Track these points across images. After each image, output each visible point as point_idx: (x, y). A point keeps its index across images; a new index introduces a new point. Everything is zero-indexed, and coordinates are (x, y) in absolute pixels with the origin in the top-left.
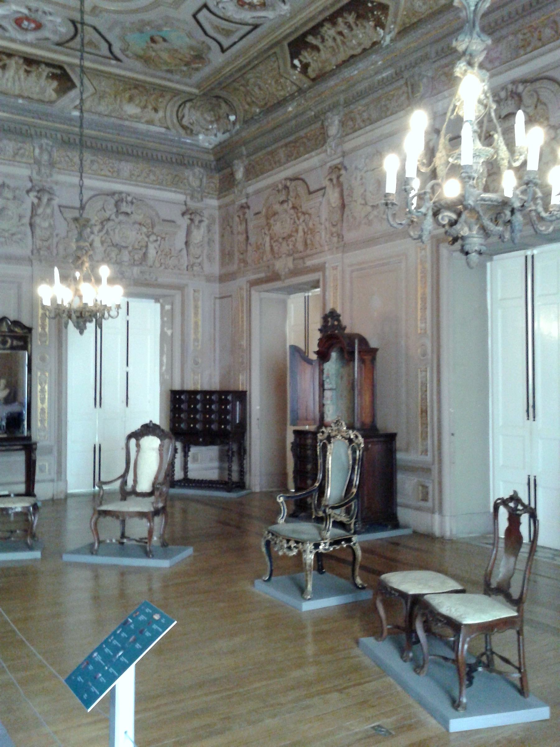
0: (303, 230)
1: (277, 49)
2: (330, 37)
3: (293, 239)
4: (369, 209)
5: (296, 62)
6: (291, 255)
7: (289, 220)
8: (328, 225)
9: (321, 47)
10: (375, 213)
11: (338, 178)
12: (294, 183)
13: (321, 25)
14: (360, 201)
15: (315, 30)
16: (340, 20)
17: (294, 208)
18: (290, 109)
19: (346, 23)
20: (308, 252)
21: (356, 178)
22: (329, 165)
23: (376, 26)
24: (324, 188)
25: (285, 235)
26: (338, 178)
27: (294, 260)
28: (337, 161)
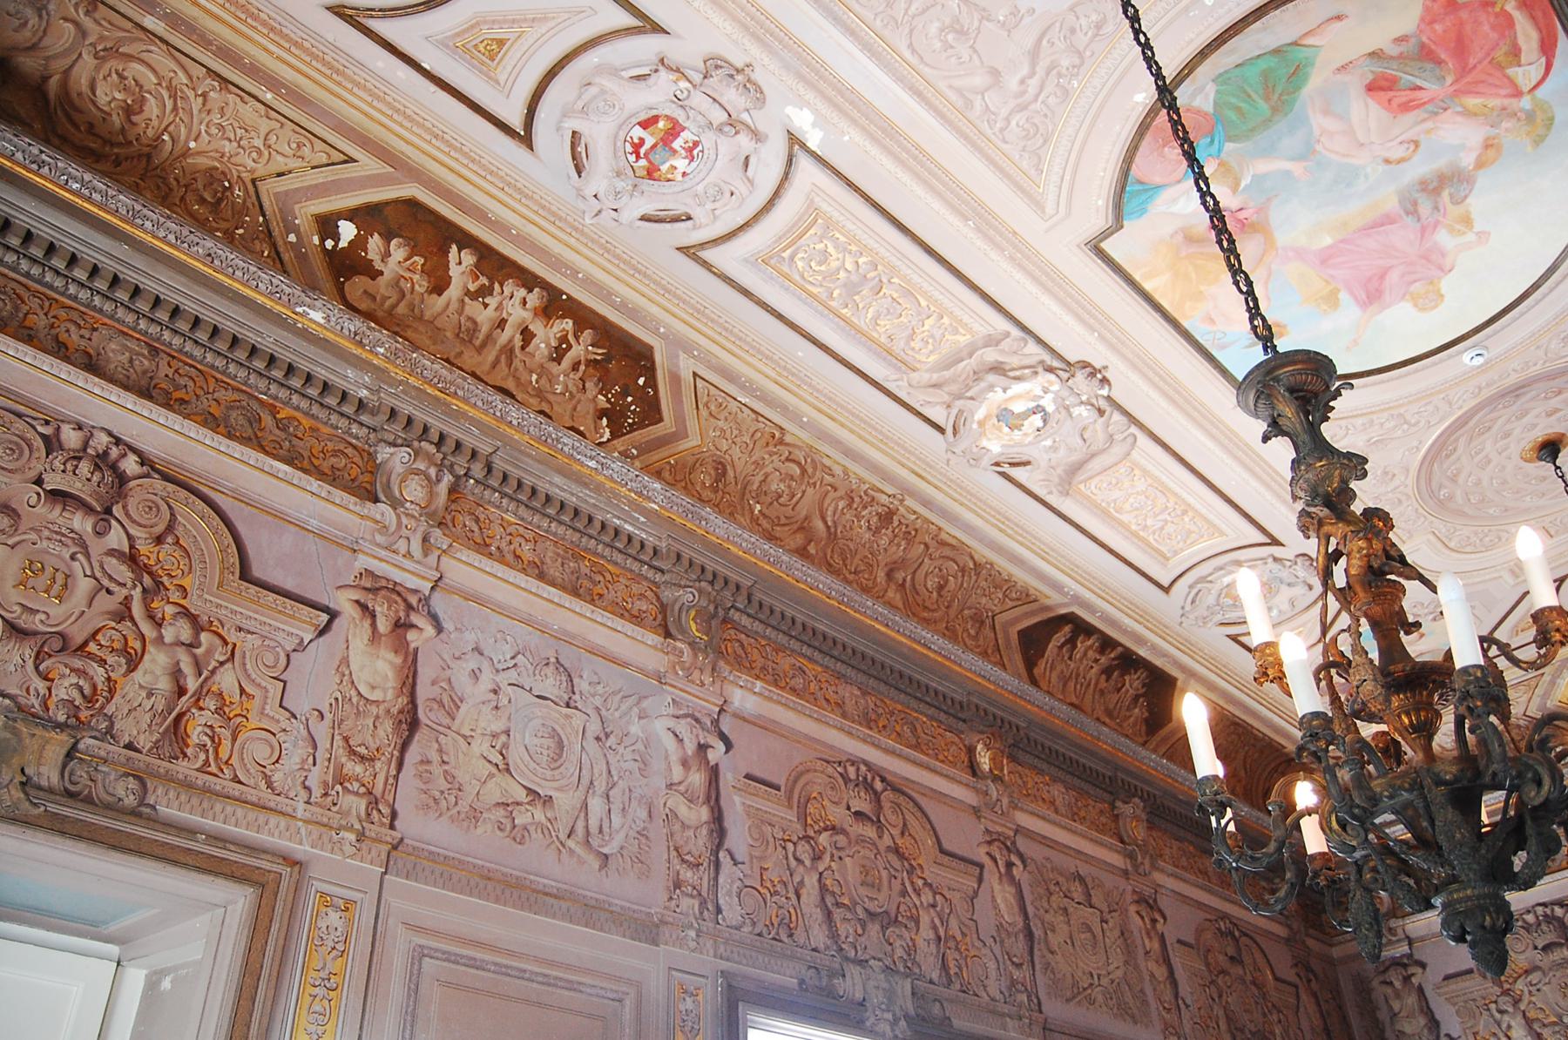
0: (176, 674)
1: (368, 164)
2: (499, 308)
3: (99, 673)
4: (521, 795)
5: (348, 231)
6: (61, 727)
7: (84, 585)
8: (321, 731)
9: (454, 292)
10: (539, 815)
11: (401, 626)
12: (158, 484)
13: (529, 281)
14: (481, 746)
15: (494, 266)
16: (568, 324)
17: (132, 558)
18: (317, 316)
19: (564, 339)
20: (183, 768)
21: (475, 675)
22: (363, 562)
23: (602, 413)
24: (333, 615)
25: (36, 623)
26: (401, 626)
27: (70, 755)
28: (411, 582)
